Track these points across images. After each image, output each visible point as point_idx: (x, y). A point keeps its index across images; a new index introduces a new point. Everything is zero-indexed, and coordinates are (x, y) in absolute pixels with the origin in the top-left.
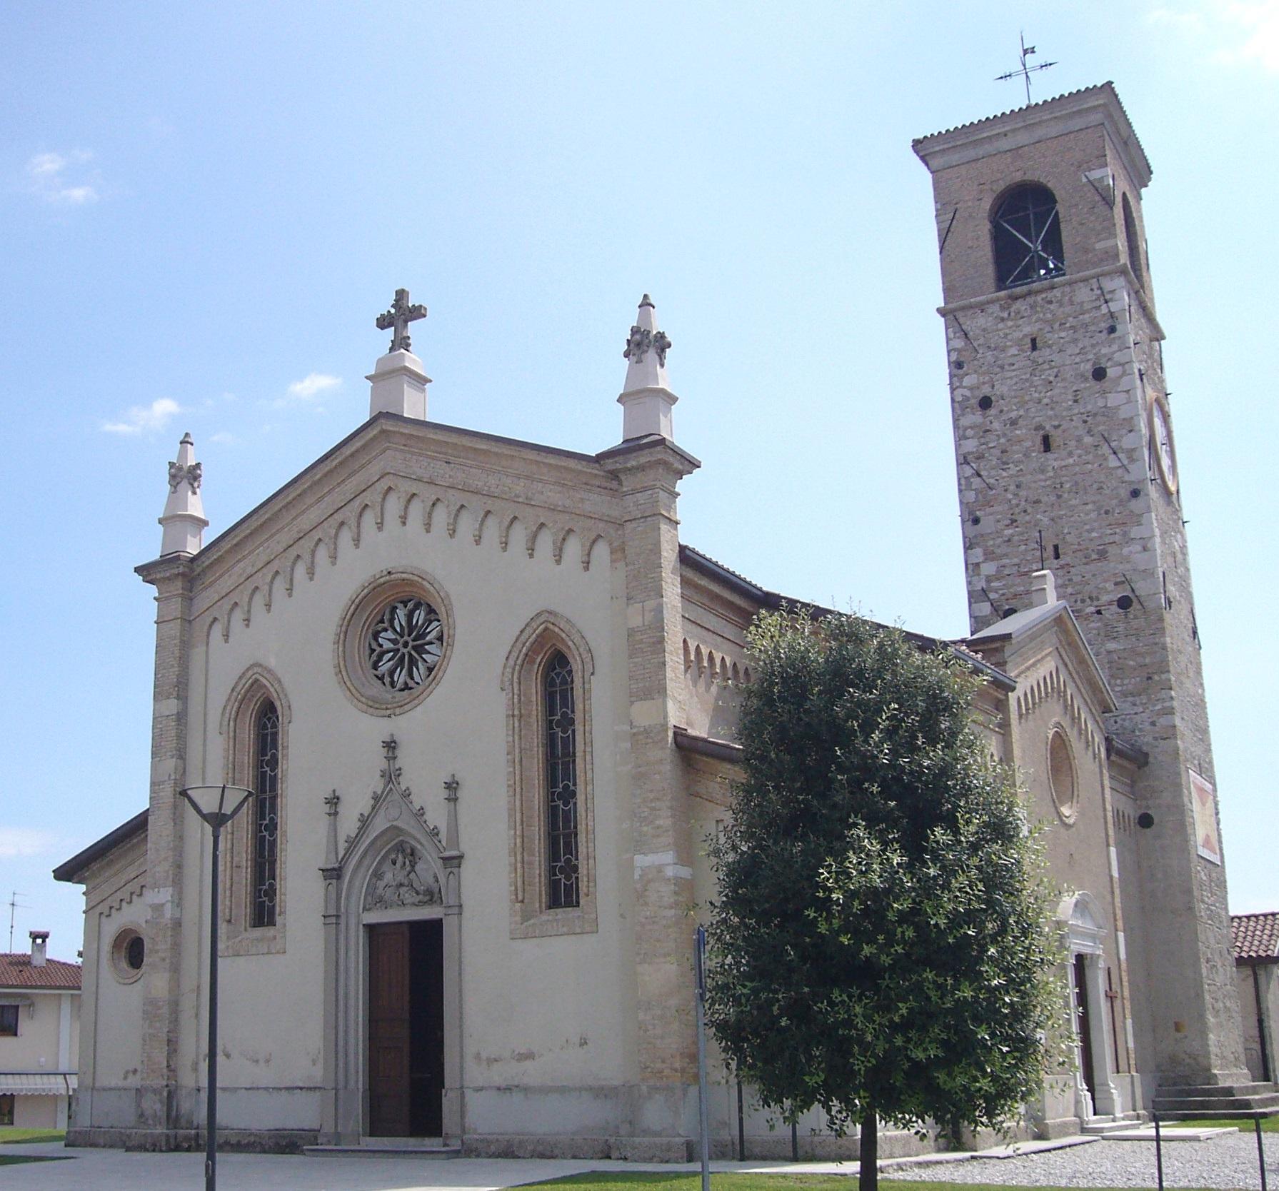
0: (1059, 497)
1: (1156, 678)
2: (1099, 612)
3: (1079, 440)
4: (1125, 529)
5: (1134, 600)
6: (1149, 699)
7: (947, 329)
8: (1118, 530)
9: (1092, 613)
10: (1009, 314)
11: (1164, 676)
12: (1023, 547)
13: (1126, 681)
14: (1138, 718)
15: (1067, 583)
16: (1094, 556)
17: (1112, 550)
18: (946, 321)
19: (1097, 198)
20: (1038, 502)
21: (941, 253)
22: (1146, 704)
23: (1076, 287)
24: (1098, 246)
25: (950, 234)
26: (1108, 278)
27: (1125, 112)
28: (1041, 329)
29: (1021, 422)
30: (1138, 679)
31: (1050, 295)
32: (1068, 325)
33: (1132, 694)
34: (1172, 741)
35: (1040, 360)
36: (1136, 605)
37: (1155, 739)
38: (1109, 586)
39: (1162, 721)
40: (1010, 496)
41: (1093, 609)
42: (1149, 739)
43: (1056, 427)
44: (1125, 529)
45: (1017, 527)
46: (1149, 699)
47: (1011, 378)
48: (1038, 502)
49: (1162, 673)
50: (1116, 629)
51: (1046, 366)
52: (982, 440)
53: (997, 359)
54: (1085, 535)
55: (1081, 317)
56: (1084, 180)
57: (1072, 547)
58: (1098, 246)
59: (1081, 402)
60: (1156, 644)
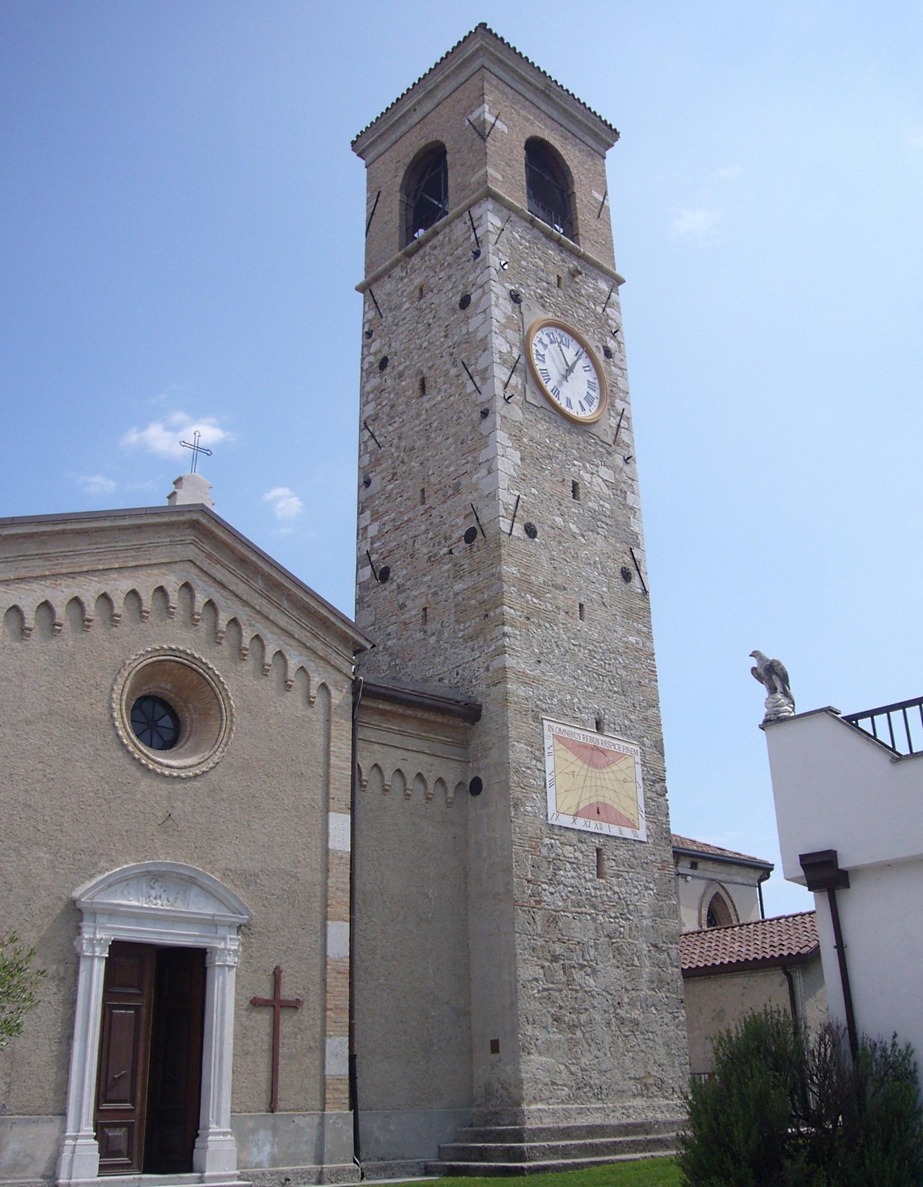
0: (428, 437)
1: (492, 614)
2: (451, 552)
3: (446, 374)
4: (475, 455)
5: (479, 531)
6: (485, 640)
7: (365, 303)
8: (470, 458)
9: (445, 555)
10: (407, 272)
11: (498, 611)
12: (399, 499)
13: (468, 624)
14: (475, 664)
15: (429, 527)
16: (450, 492)
17: (464, 481)
18: (364, 297)
19: (476, 135)
20: (412, 449)
21: (366, 236)
22: (482, 647)
23: (453, 225)
24: (472, 181)
25: (374, 217)
26: (477, 206)
27: (502, 39)
28: (427, 277)
29: (406, 373)
30: (477, 620)
31: (434, 242)
32: (446, 264)
33: (471, 638)
34: (502, 685)
35: (424, 306)
36: (479, 536)
37: (488, 686)
38: (460, 521)
39: (496, 664)
40: (393, 450)
41: (445, 550)
42: (483, 687)
43: (430, 368)
44: (475, 455)
45: (397, 480)
46: (485, 640)
47: (402, 333)
48: (412, 449)
49: (496, 607)
50: (462, 568)
51: (428, 311)
52: (378, 401)
53: (395, 317)
54: (445, 470)
55: (456, 252)
56: (467, 123)
57: (435, 487)
58: (472, 181)
59: (450, 336)
60: (493, 575)
